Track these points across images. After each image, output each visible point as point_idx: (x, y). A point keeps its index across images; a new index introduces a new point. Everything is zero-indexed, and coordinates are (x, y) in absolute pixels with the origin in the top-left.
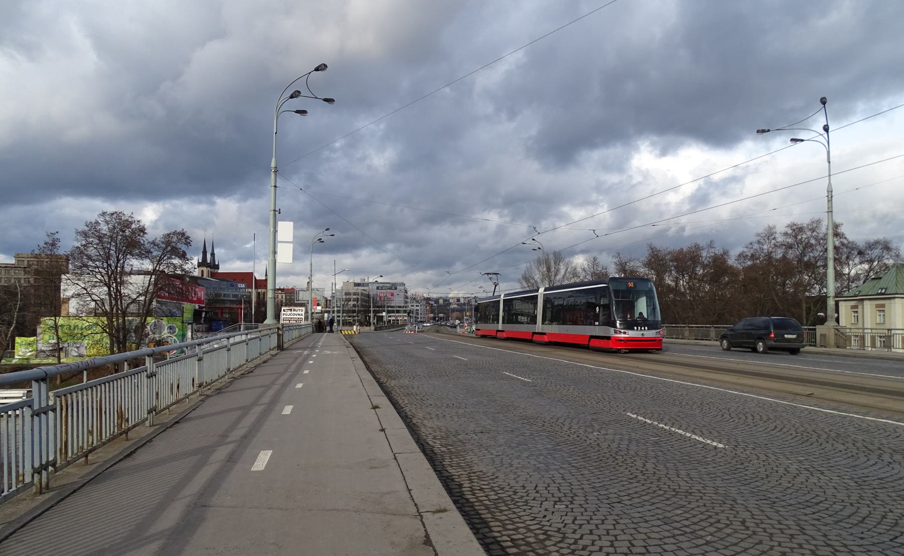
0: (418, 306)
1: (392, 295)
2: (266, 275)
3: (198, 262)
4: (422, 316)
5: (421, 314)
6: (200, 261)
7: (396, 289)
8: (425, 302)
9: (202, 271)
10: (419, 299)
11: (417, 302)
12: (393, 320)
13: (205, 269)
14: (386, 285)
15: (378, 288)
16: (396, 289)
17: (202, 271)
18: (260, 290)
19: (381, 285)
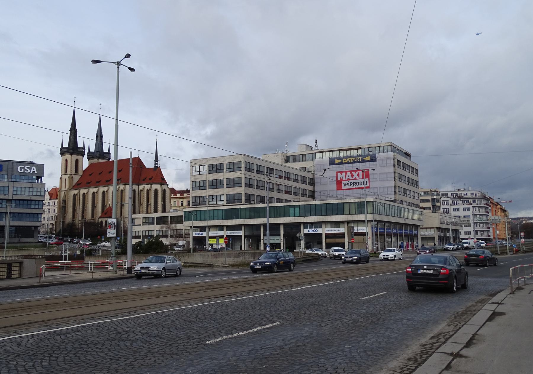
0: (468, 209)
1: (366, 174)
2: (156, 161)
3: (62, 147)
4: (478, 228)
5: (476, 224)
6: (66, 145)
7: (373, 159)
8: (483, 202)
9: (66, 160)
10: (469, 195)
11: (466, 201)
12: (328, 236)
13: (68, 157)
14: (352, 153)
15: (332, 162)
16: (373, 159)
17: (66, 160)
18: (141, 187)
19: (342, 154)
